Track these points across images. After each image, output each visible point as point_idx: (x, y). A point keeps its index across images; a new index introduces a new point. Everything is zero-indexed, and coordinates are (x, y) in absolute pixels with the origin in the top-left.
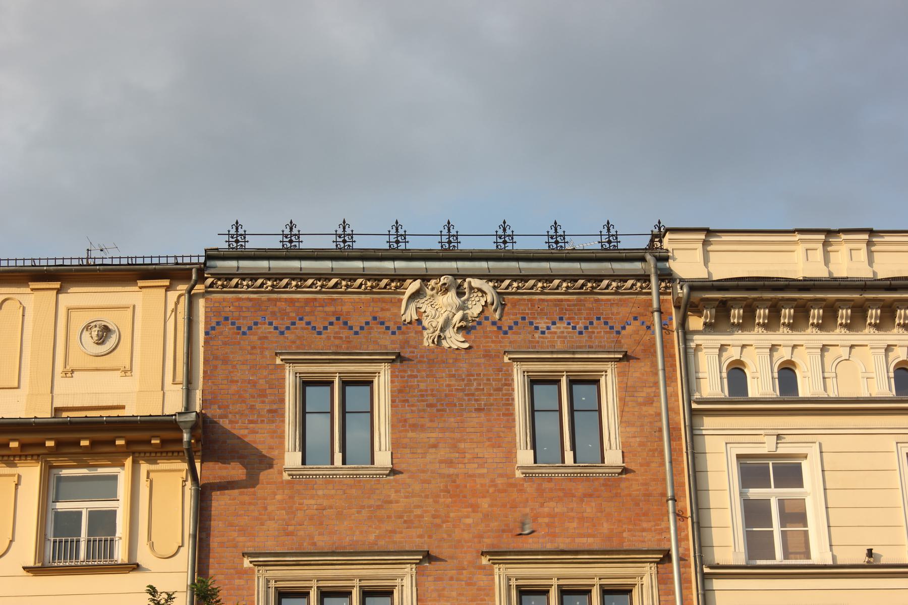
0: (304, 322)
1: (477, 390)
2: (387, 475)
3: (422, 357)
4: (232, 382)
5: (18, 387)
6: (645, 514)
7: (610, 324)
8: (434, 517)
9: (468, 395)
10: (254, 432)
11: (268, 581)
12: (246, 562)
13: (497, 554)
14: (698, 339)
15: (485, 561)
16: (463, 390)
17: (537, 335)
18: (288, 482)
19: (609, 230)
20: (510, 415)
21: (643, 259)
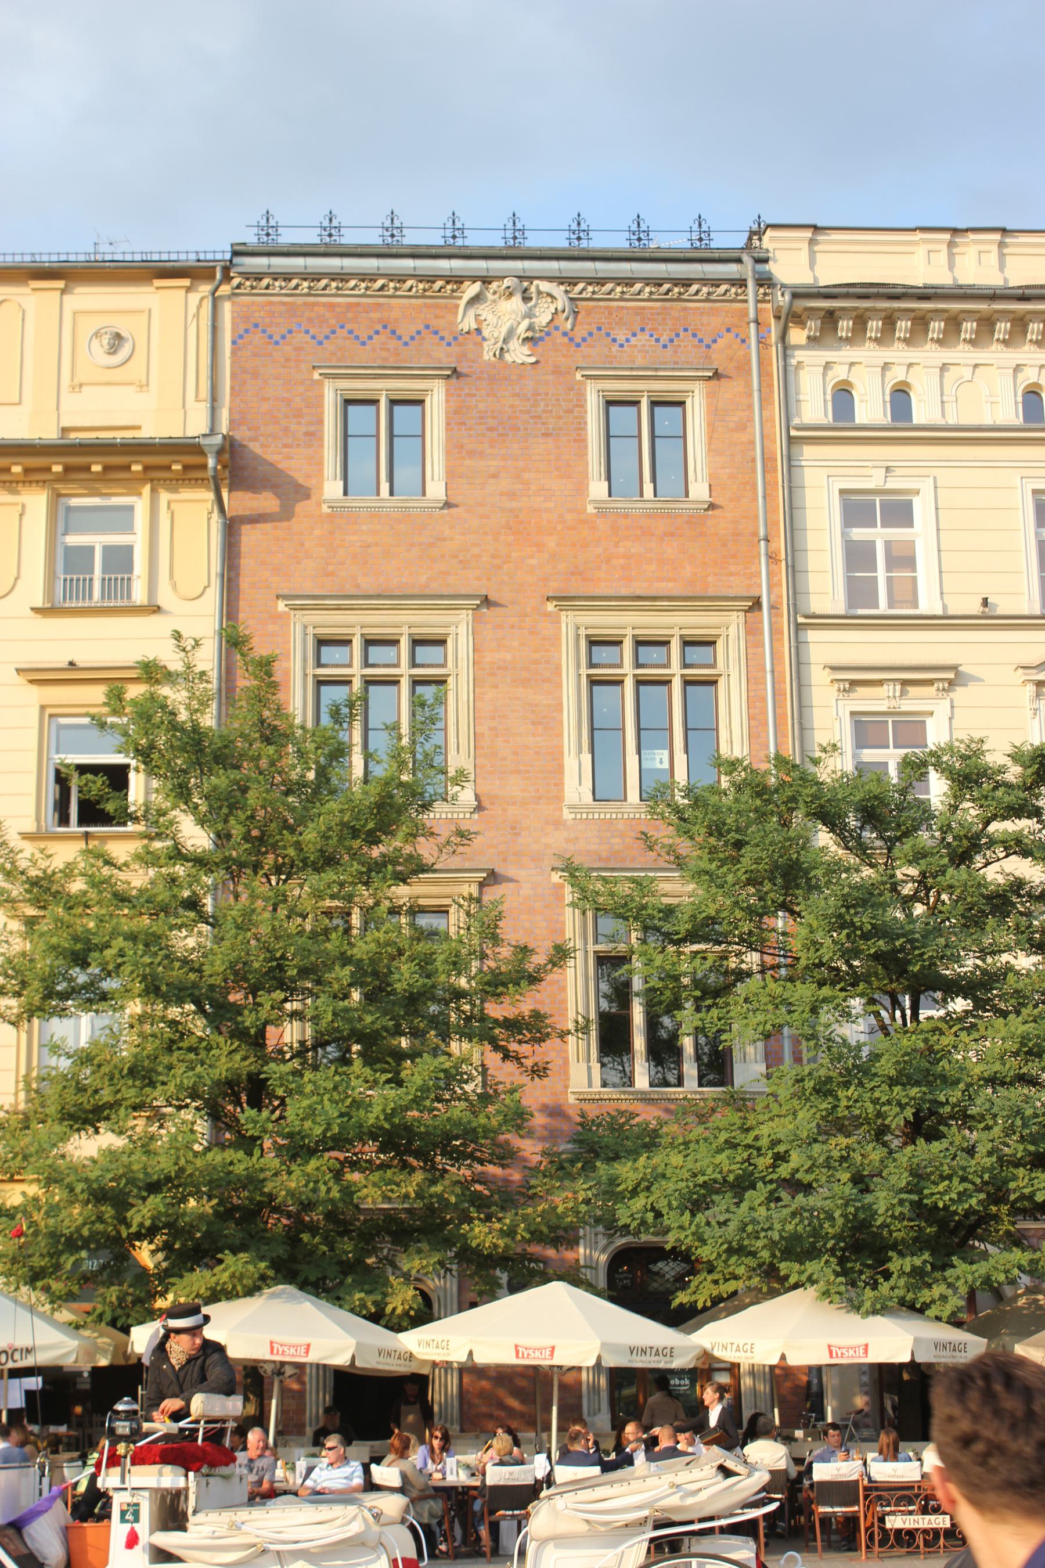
0: (345, 330)
1: (545, 411)
2: (441, 508)
3: (482, 372)
4: (265, 399)
5: (20, 403)
6: (734, 556)
7: (699, 336)
8: (494, 557)
9: (535, 417)
10: (288, 457)
11: (305, 627)
12: (281, 606)
13: (564, 600)
14: (799, 356)
15: (550, 607)
16: (528, 412)
17: (615, 348)
18: (328, 515)
19: (700, 225)
20: (581, 441)
21: (739, 261)
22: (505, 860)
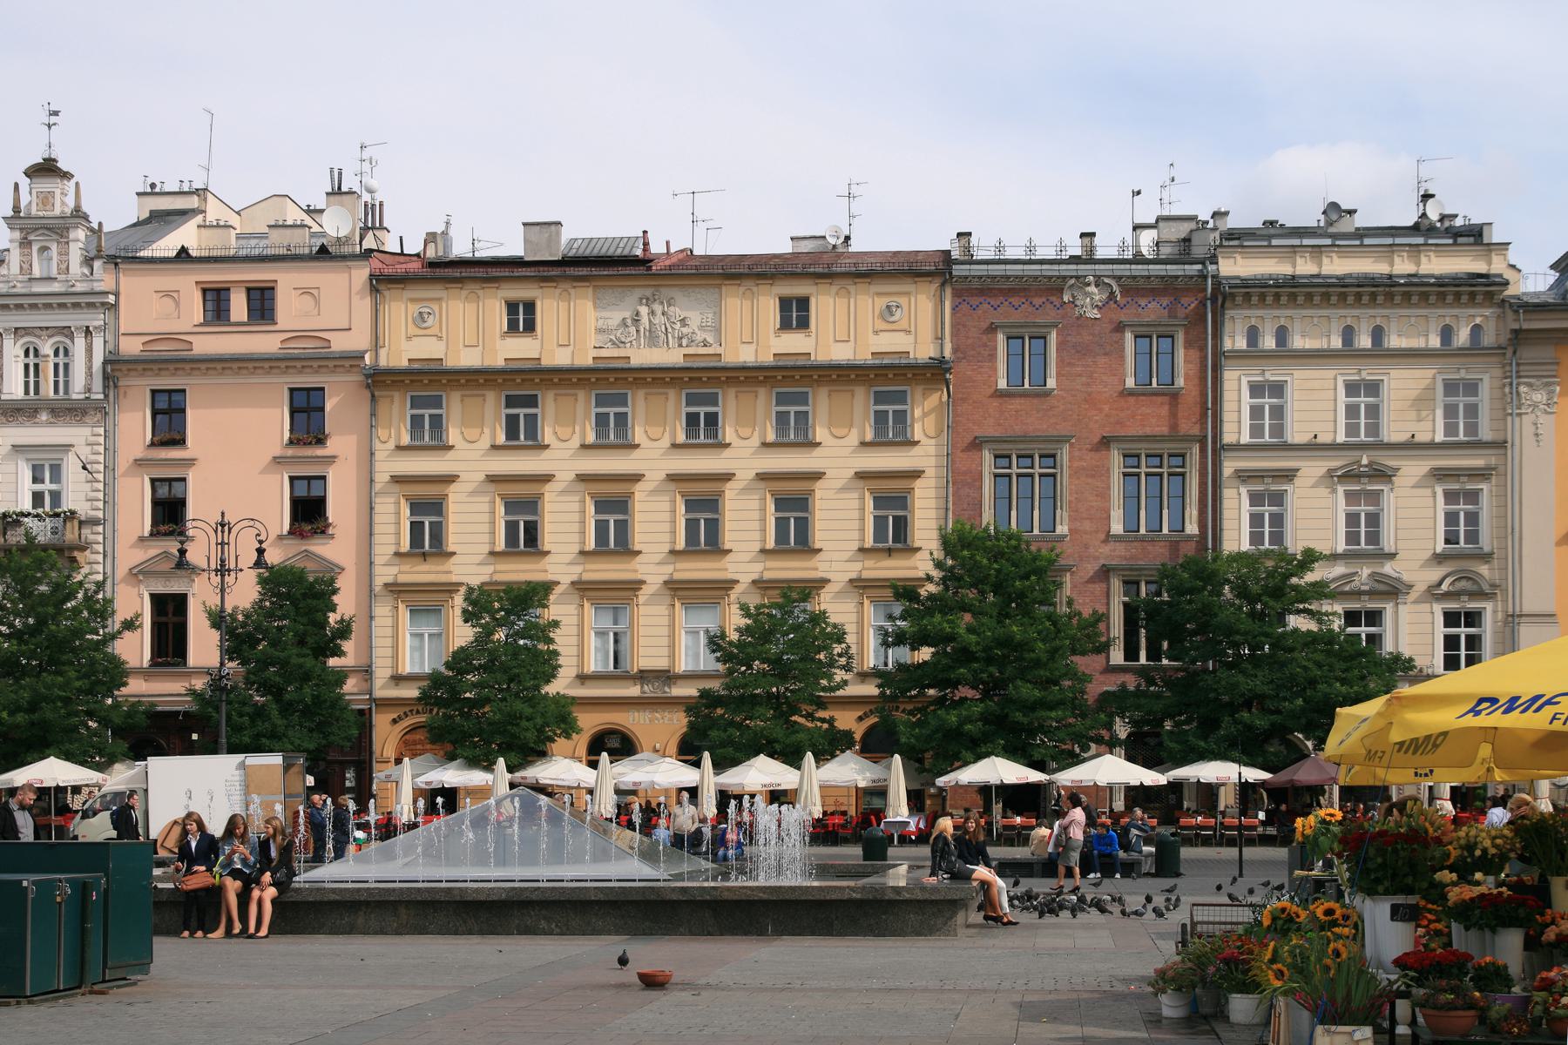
17: (1140, 309)
20: (1122, 357)
22: (1082, 560)
